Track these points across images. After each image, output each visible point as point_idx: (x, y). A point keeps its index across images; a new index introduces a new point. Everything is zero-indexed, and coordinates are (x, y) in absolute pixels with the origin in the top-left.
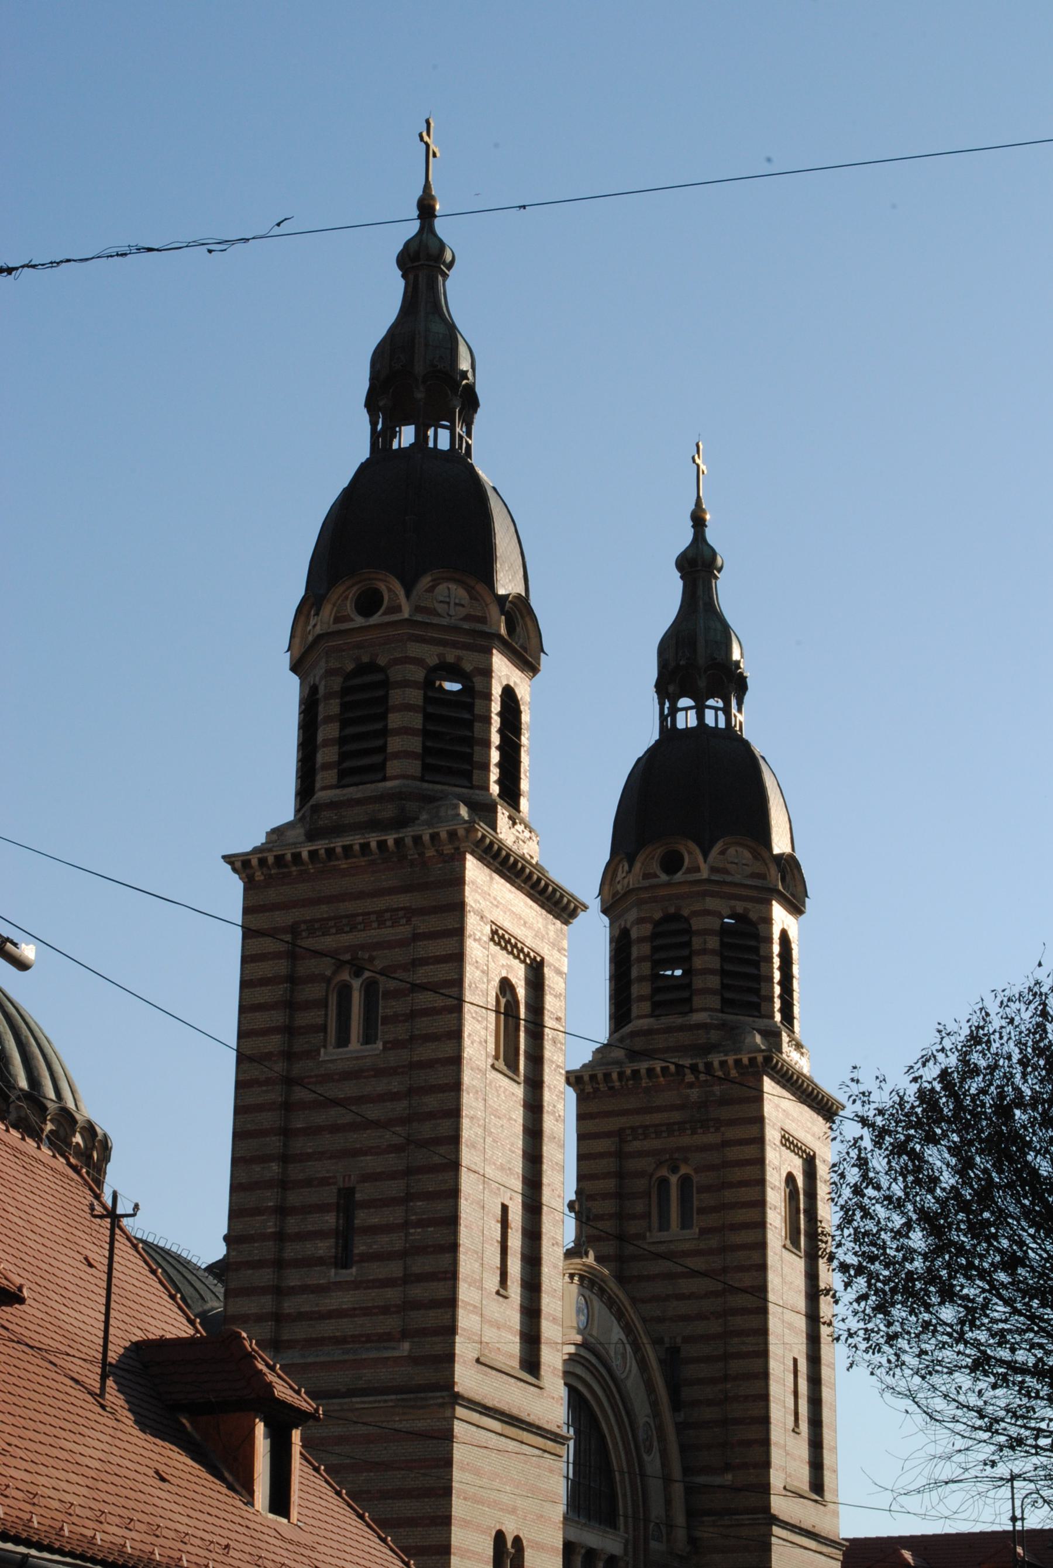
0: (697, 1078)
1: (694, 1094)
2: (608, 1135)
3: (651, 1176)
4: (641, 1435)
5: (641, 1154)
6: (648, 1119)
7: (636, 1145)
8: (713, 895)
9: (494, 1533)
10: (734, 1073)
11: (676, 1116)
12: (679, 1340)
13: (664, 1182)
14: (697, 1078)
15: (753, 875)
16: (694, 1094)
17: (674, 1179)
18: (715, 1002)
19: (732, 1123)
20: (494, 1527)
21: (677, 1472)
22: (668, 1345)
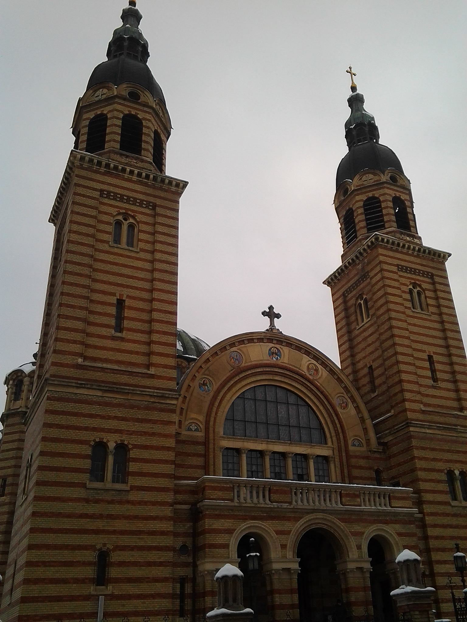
0: (360, 260)
1: (360, 267)
2: (340, 297)
3: (355, 305)
4: (336, 401)
5: (351, 298)
6: (349, 285)
7: (350, 296)
8: (358, 195)
9: (92, 443)
10: (369, 251)
11: (356, 278)
12: (371, 362)
13: (360, 304)
14: (360, 260)
15: (374, 182)
16: (360, 267)
17: (362, 302)
18: (365, 231)
19: (372, 269)
20: (94, 440)
21: (366, 415)
22: (368, 366)
